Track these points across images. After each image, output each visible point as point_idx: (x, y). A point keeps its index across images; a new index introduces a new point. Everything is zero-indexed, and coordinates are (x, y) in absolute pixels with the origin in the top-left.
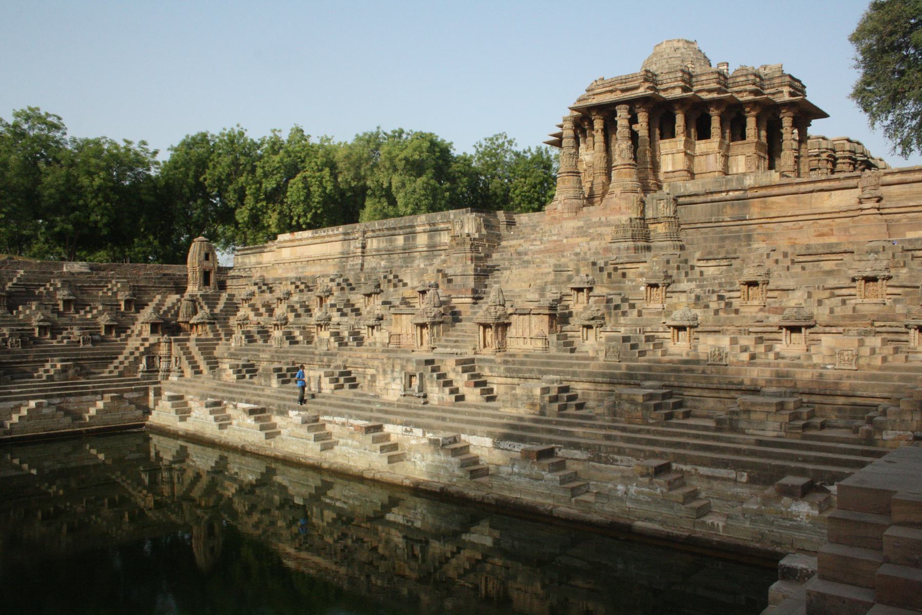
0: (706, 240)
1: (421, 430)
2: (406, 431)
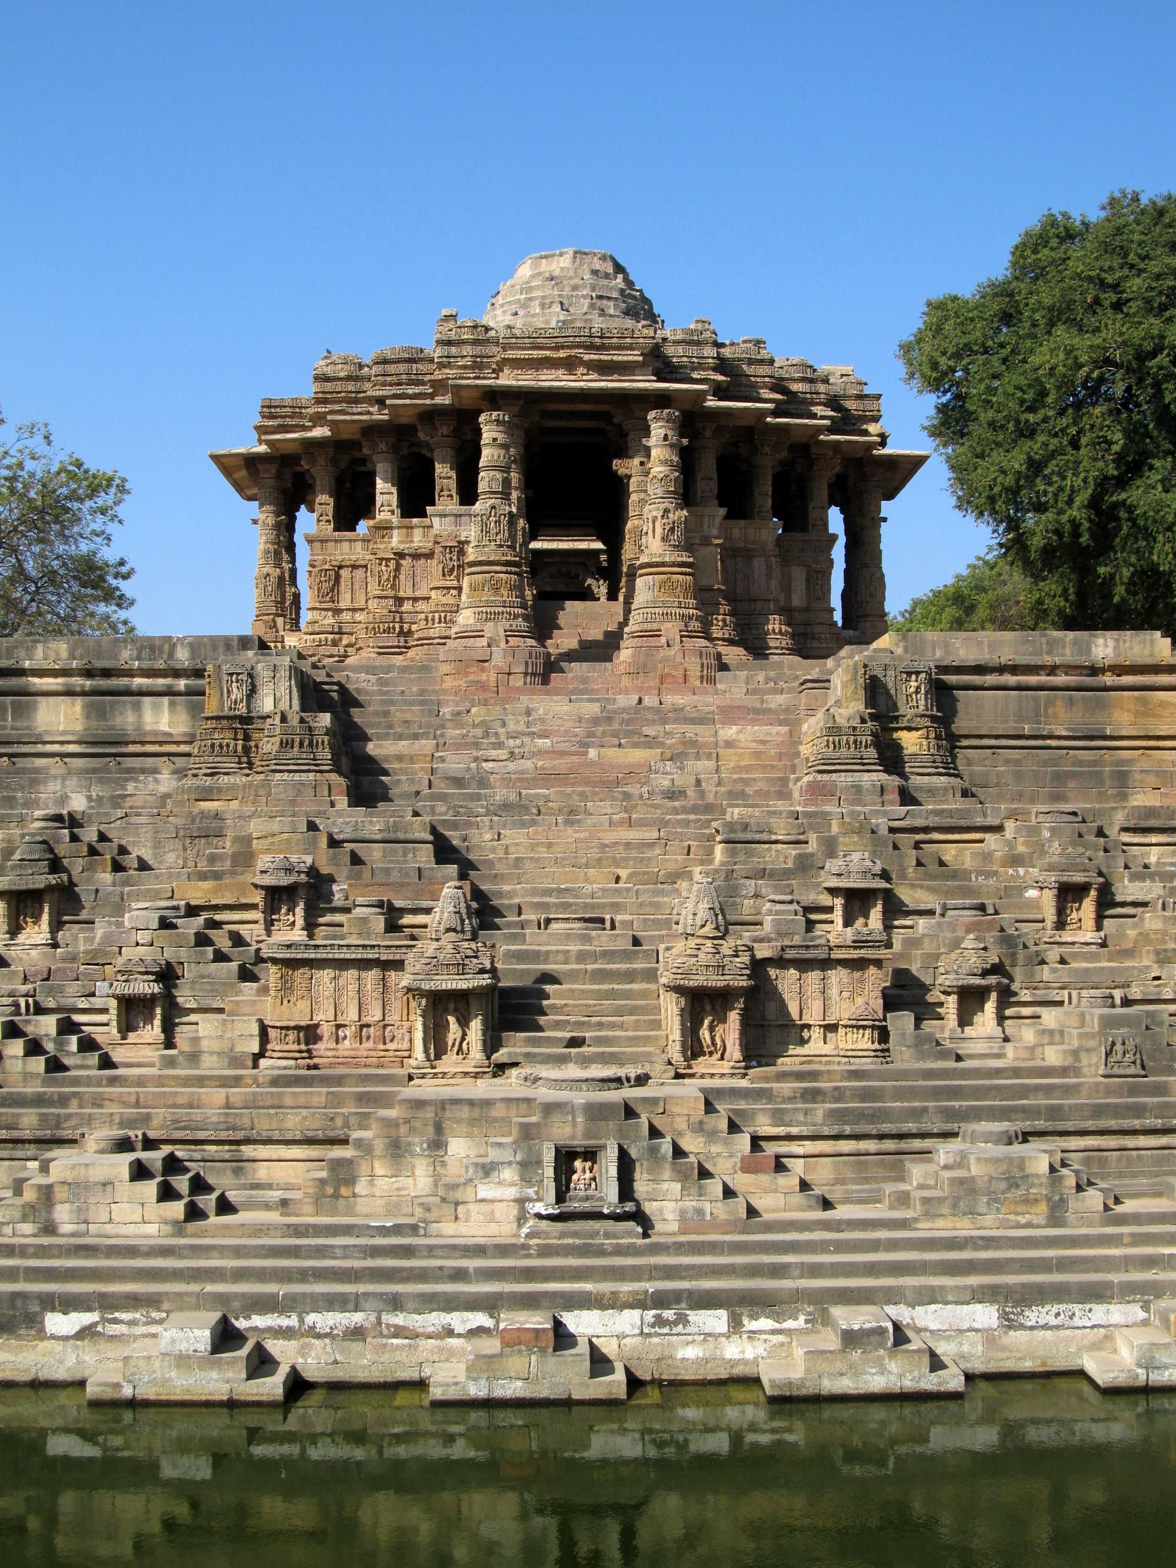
0: (1018, 776)
1: (723, 1314)
2: (660, 1321)
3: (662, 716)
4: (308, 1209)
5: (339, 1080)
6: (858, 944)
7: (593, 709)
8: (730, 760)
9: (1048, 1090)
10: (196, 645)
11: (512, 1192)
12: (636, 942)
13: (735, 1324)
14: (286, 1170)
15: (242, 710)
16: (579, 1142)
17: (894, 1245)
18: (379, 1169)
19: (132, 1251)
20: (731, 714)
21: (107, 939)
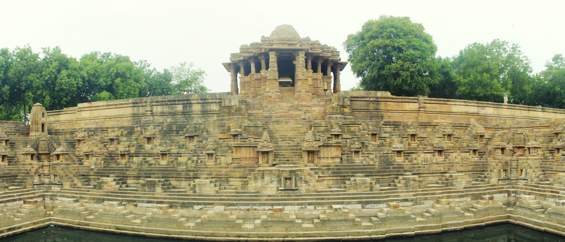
2: (302, 208)
3: (302, 106)
4: (240, 189)
5: (246, 167)
6: (337, 143)
7: (290, 105)
8: (314, 113)
9: (370, 168)
10: (220, 94)
11: (276, 186)
12: (298, 144)
13: (315, 208)
14: (236, 183)
15: (229, 105)
16: (288, 177)
17: (343, 194)
18: (252, 182)
19: (209, 196)
20: (315, 105)
21: (205, 144)
